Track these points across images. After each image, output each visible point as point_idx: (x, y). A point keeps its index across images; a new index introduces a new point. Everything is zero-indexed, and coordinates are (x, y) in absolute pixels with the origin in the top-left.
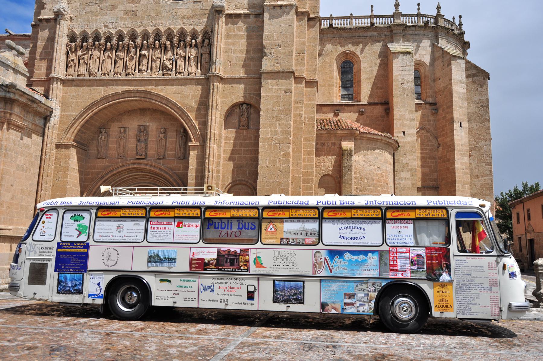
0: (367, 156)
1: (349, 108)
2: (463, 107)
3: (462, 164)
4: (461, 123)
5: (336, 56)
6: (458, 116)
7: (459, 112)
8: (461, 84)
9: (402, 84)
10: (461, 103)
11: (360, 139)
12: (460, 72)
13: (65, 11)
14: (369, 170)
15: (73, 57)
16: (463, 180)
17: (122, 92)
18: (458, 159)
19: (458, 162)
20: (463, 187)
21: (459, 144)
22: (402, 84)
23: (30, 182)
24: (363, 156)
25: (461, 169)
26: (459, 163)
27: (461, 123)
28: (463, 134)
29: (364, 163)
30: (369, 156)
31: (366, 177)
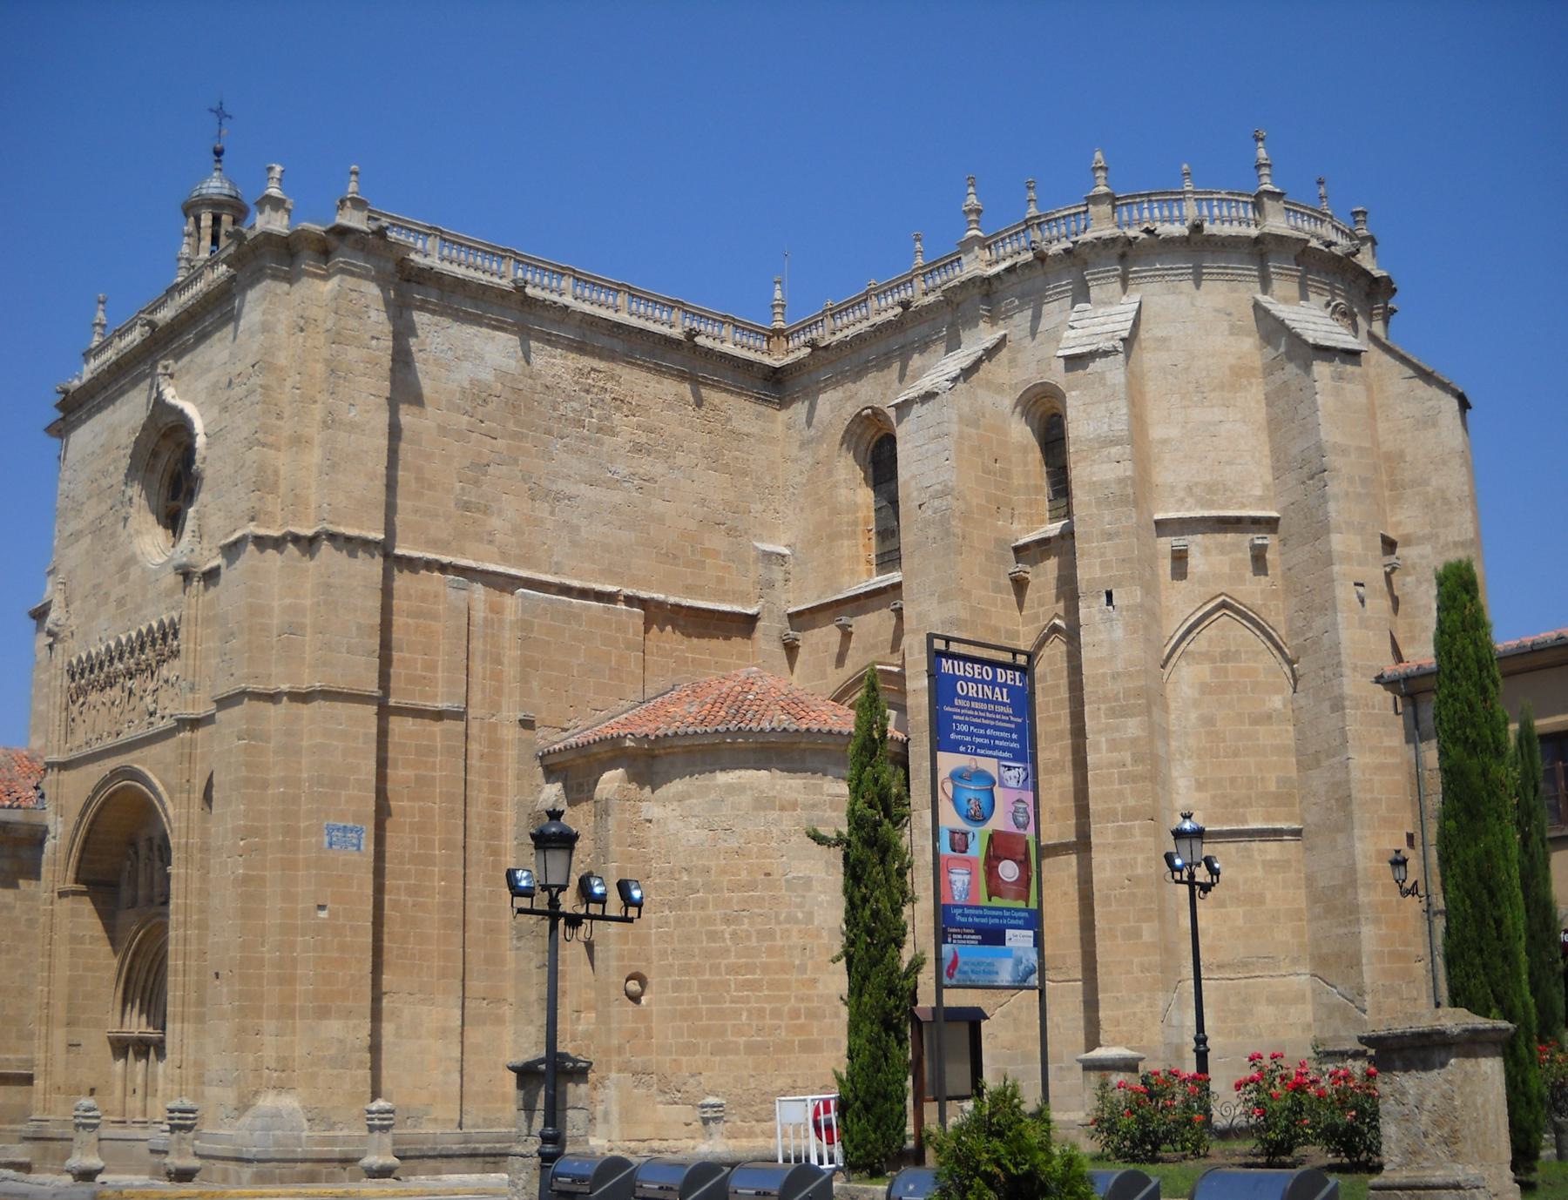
0: (687, 802)
1: (875, 601)
2: (1117, 534)
3: (1114, 745)
4: (1109, 595)
5: (840, 436)
6: (1097, 573)
7: (1102, 555)
8: (1105, 452)
9: (920, 506)
10: (1107, 519)
11: (668, 754)
12: (1103, 407)
13: (57, 625)
14: (693, 843)
15: (75, 709)
16: (1119, 807)
17: (111, 772)
18: (1100, 732)
19: (1098, 743)
20: (1123, 832)
21: (1104, 675)
22: (920, 506)
23: (20, 971)
24: (676, 803)
25: (1111, 765)
26: (1104, 747)
27: (1109, 595)
28: (1119, 633)
29: (680, 824)
30: (695, 801)
31: (684, 864)
